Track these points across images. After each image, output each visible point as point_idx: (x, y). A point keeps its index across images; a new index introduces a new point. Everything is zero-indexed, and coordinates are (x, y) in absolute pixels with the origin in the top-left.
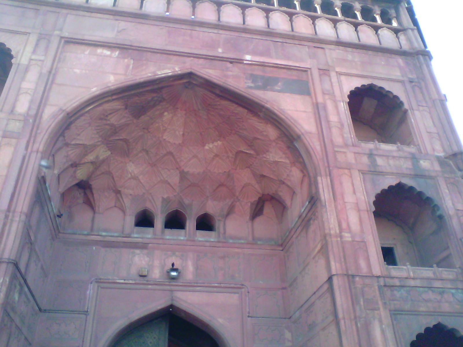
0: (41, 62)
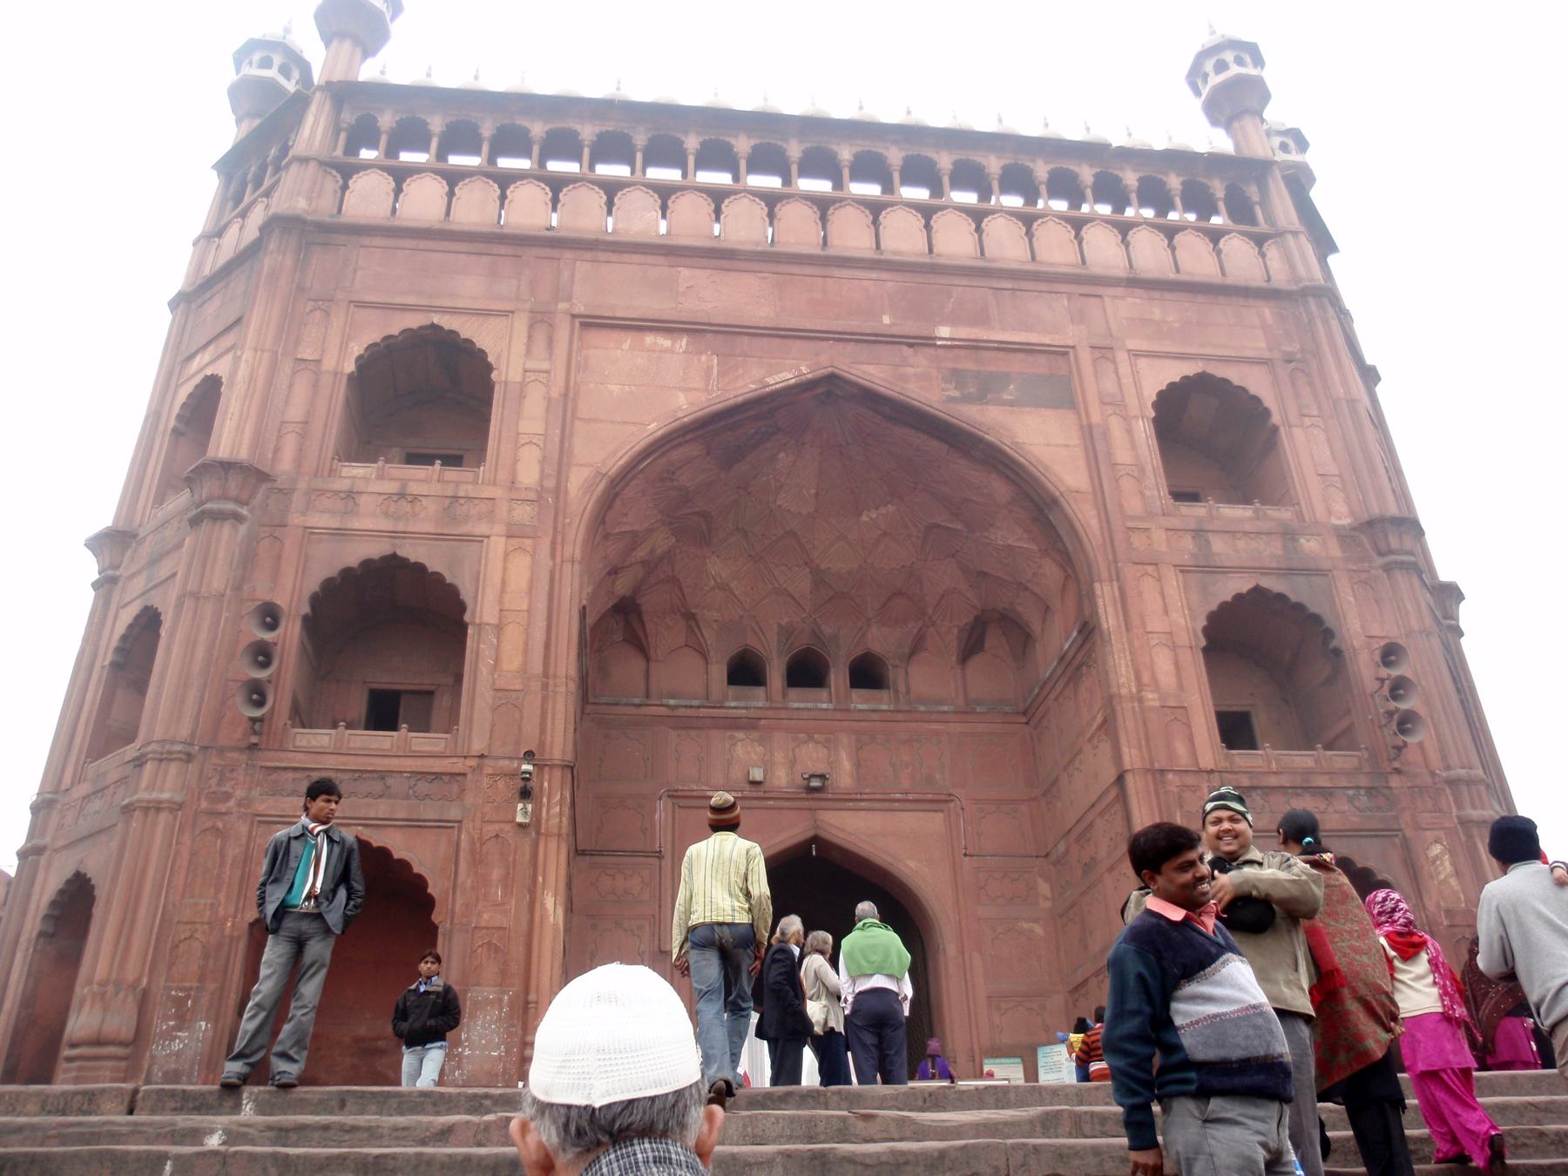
0: (545, 375)
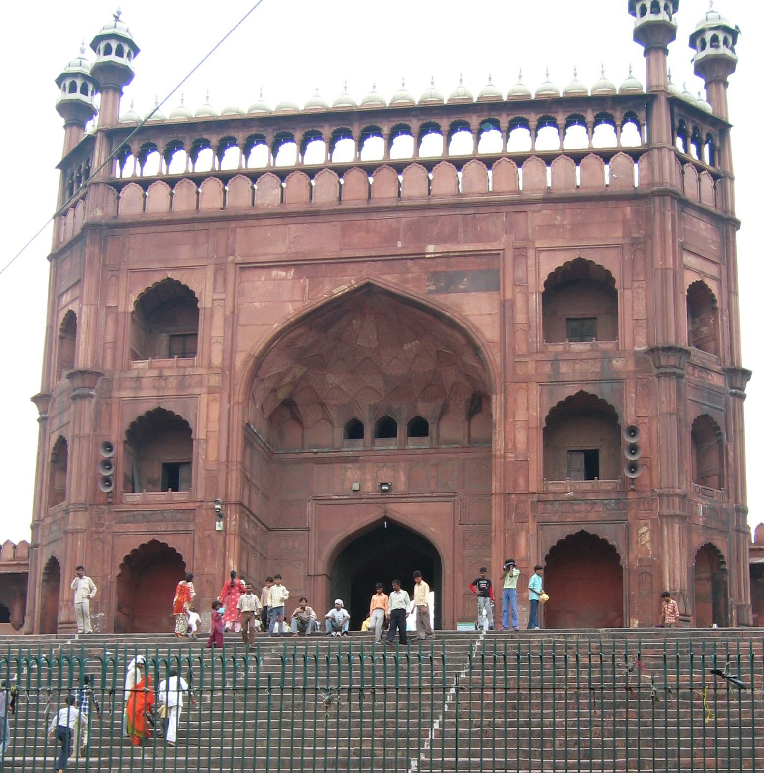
0: (223, 302)
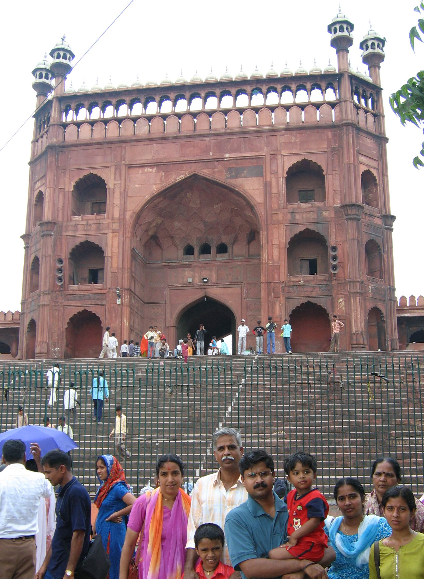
0: (119, 185)
